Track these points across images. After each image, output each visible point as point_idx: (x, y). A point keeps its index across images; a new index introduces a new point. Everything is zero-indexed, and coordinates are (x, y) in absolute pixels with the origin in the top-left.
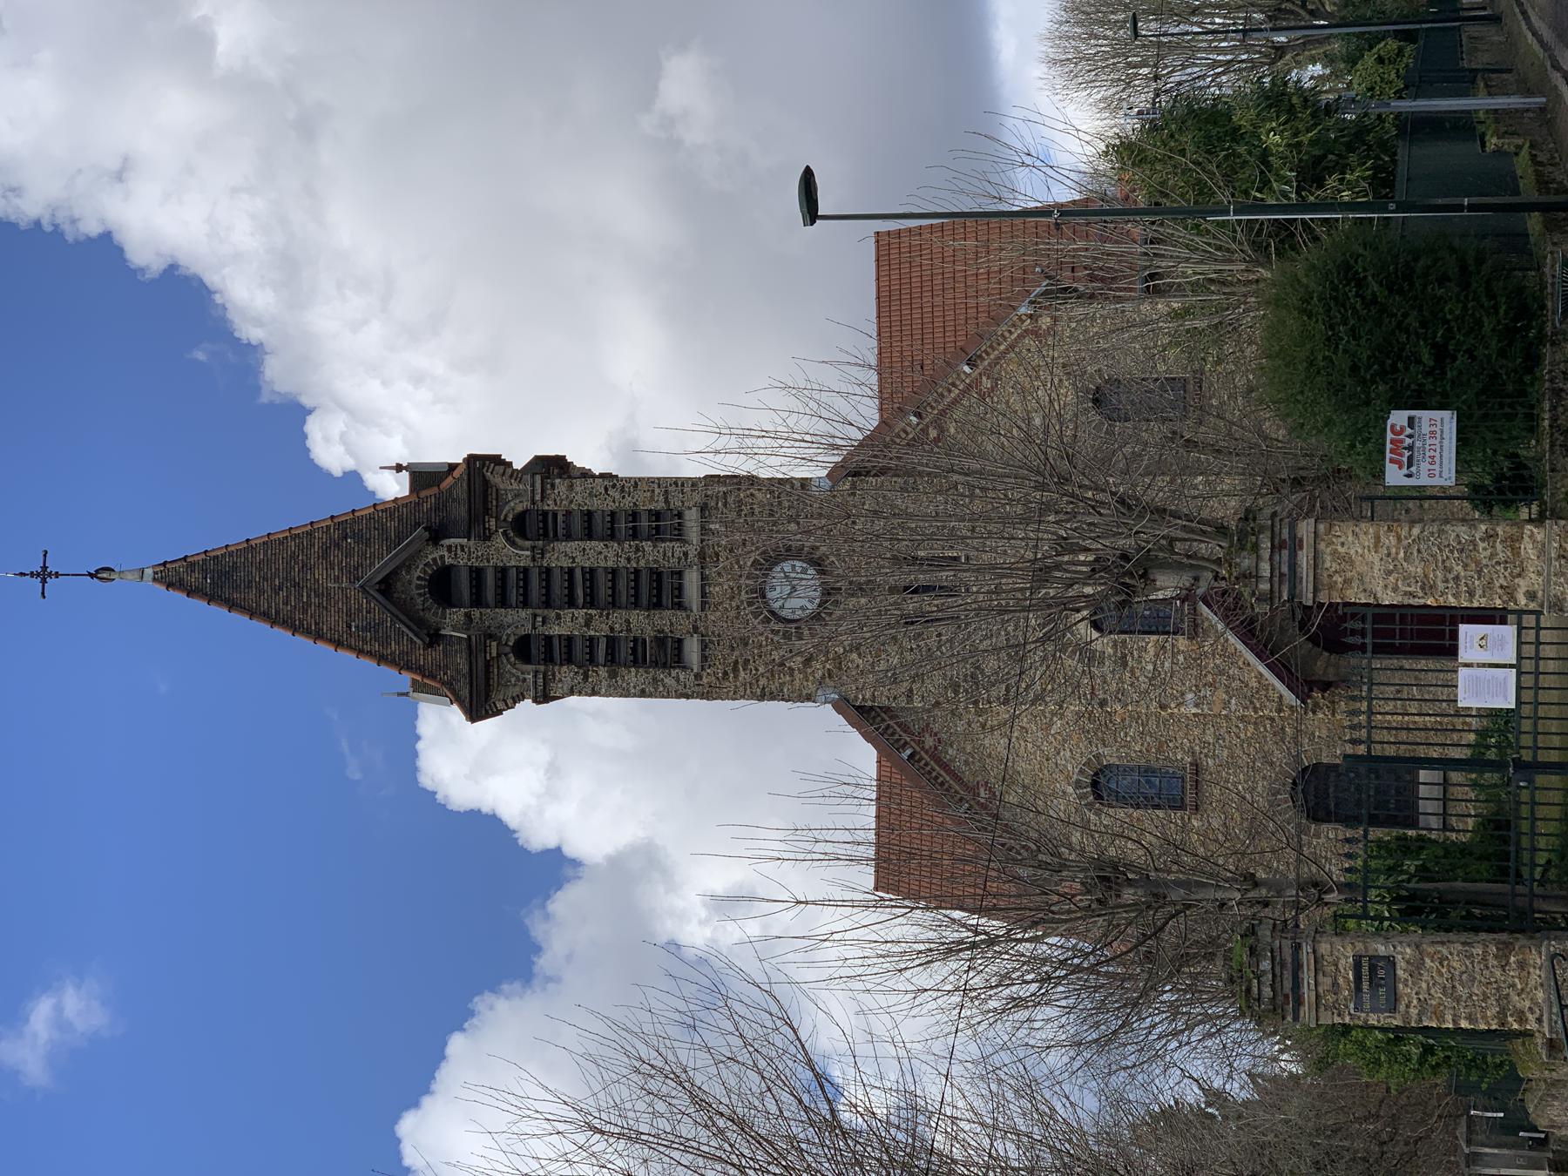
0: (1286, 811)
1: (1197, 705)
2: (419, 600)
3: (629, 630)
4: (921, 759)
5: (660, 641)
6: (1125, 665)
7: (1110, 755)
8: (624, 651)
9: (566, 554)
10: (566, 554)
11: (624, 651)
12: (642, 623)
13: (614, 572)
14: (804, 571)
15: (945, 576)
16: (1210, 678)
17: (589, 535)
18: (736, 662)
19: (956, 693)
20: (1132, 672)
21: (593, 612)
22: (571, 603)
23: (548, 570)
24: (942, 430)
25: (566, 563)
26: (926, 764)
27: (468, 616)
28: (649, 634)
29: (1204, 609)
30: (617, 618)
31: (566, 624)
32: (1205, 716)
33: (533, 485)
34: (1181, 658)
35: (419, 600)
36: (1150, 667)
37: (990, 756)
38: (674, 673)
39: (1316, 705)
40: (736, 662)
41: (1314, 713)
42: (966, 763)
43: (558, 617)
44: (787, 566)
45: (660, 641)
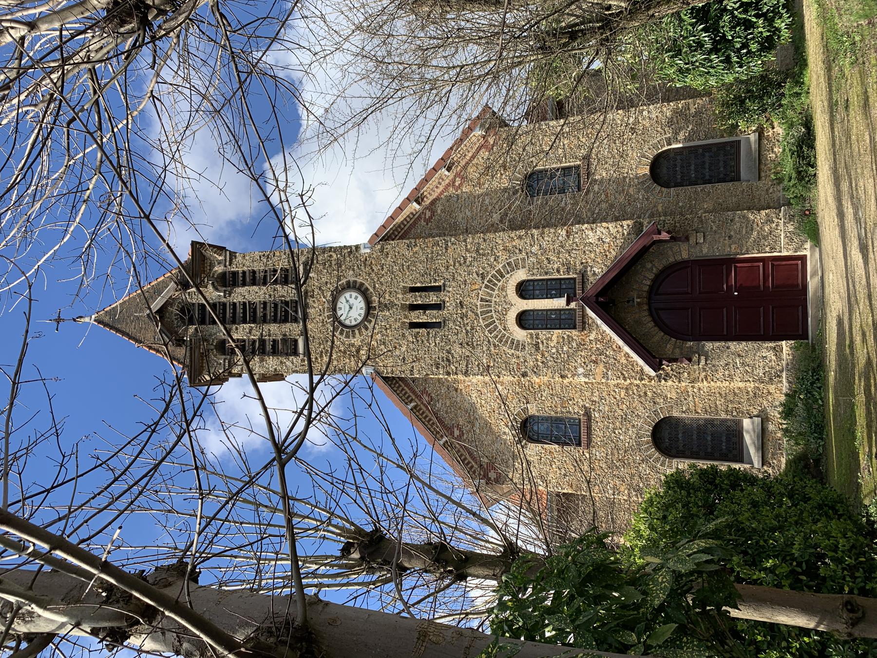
0: (647, 449)
1: (585, 376)
2: (175, 322)
3: (269, 336)
4: (420, 409)
5: (285, 340)
6: (537, 348)
7: (533, 410)
8: (269, 347)
9: (242, 294)
10: (242, 294)
11: (269, 347)
12: (275, 330)
13: (265, 303)
14: (356, 298)
15: (433, 298)
16: (593, 357)
17: (254, 283)
18: (322, 352)
19: (438, 368)
20: (543, 355)
21: (253, 325)
22: (245, 322)
23: (234, 304)
24: (433, 213)
25: (240, 299)
26: (423, 413)
27: (196, 329)
28: (280, 337)
29: (589, 312)
30: (266, 327)
31: (241, 332)
32: (592, 384)
33: (225, 257)
34: (574, 345)
35: (175, 322)
36: (554, 350)
37: (460, 408)
38: (291, 358)
39: (667, 375)
40: (322, 352)
41: (666, 380)
42: (447, 412)
43: (237, 329)
44: (347, 295)
45: (285, 340)
